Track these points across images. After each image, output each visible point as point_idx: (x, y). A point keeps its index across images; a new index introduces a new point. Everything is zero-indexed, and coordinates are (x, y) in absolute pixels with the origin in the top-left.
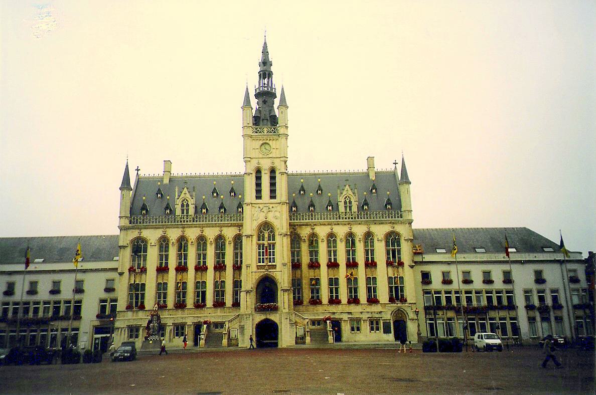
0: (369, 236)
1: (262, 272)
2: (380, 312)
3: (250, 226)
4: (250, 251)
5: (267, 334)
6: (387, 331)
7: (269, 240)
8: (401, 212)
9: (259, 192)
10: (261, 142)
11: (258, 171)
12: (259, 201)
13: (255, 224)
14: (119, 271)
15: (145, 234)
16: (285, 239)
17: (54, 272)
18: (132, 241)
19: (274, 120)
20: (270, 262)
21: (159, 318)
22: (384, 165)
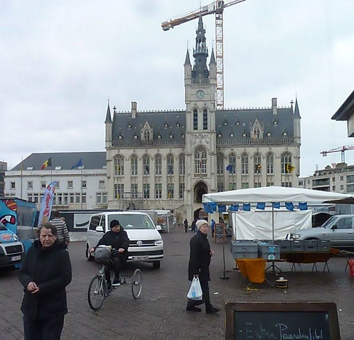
0: (270, 154)
1: (199, 179)
3: (190, 148)
4: (190, 162)
7: (203, 157)
8: (293, 138)
9: (196, 125)
10: (197, 90)
11: (195, 111)
12: (196, 131)
13: (193, 146)
14: (108, 176)
16: (213, 157)
19: (206, 74)
20: (203, 172)
22: (284, 103)
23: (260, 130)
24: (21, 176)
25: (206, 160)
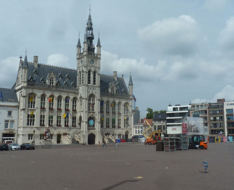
5: (91, 139)
9: (89, 81)
10: (91, 59)
11: (89, 72)
15: (35, 91)
20: (92, 110)
23: (114, 88)
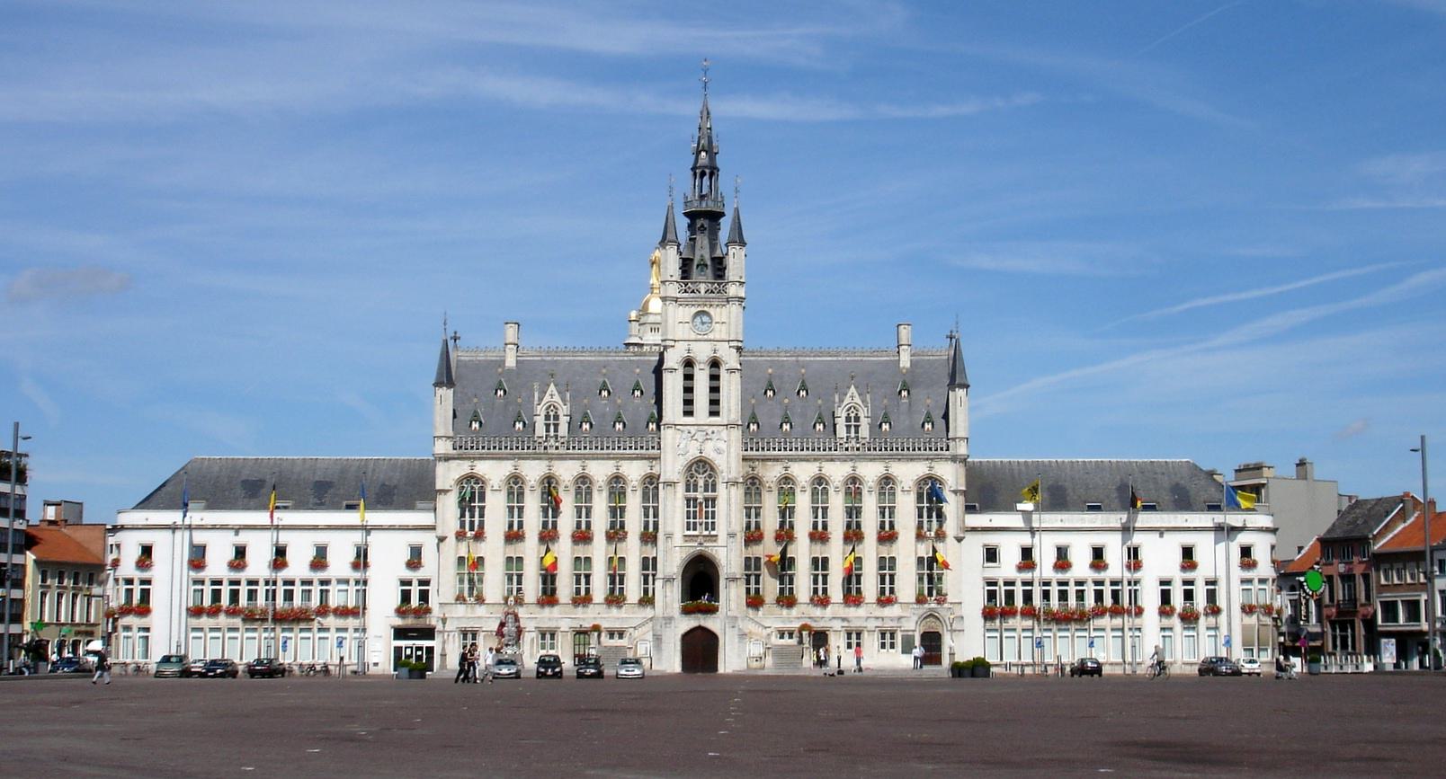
0: (887, 480)
1: (693, 548)
2: (900, 618)
4: (673, 509)
6: (907, 649)
7: (706, 490)
10: (694, 310)
11: (689, 363)
12: (689, 420)
13: (681, 463)
14: (439, 532)
15: (483, 468)
16: (733, 489)
17: (315, 528)
18: (460, 481)
21: (517, 619)
23: (861, 415)
24: (173, 528)
25: (714, 500)
